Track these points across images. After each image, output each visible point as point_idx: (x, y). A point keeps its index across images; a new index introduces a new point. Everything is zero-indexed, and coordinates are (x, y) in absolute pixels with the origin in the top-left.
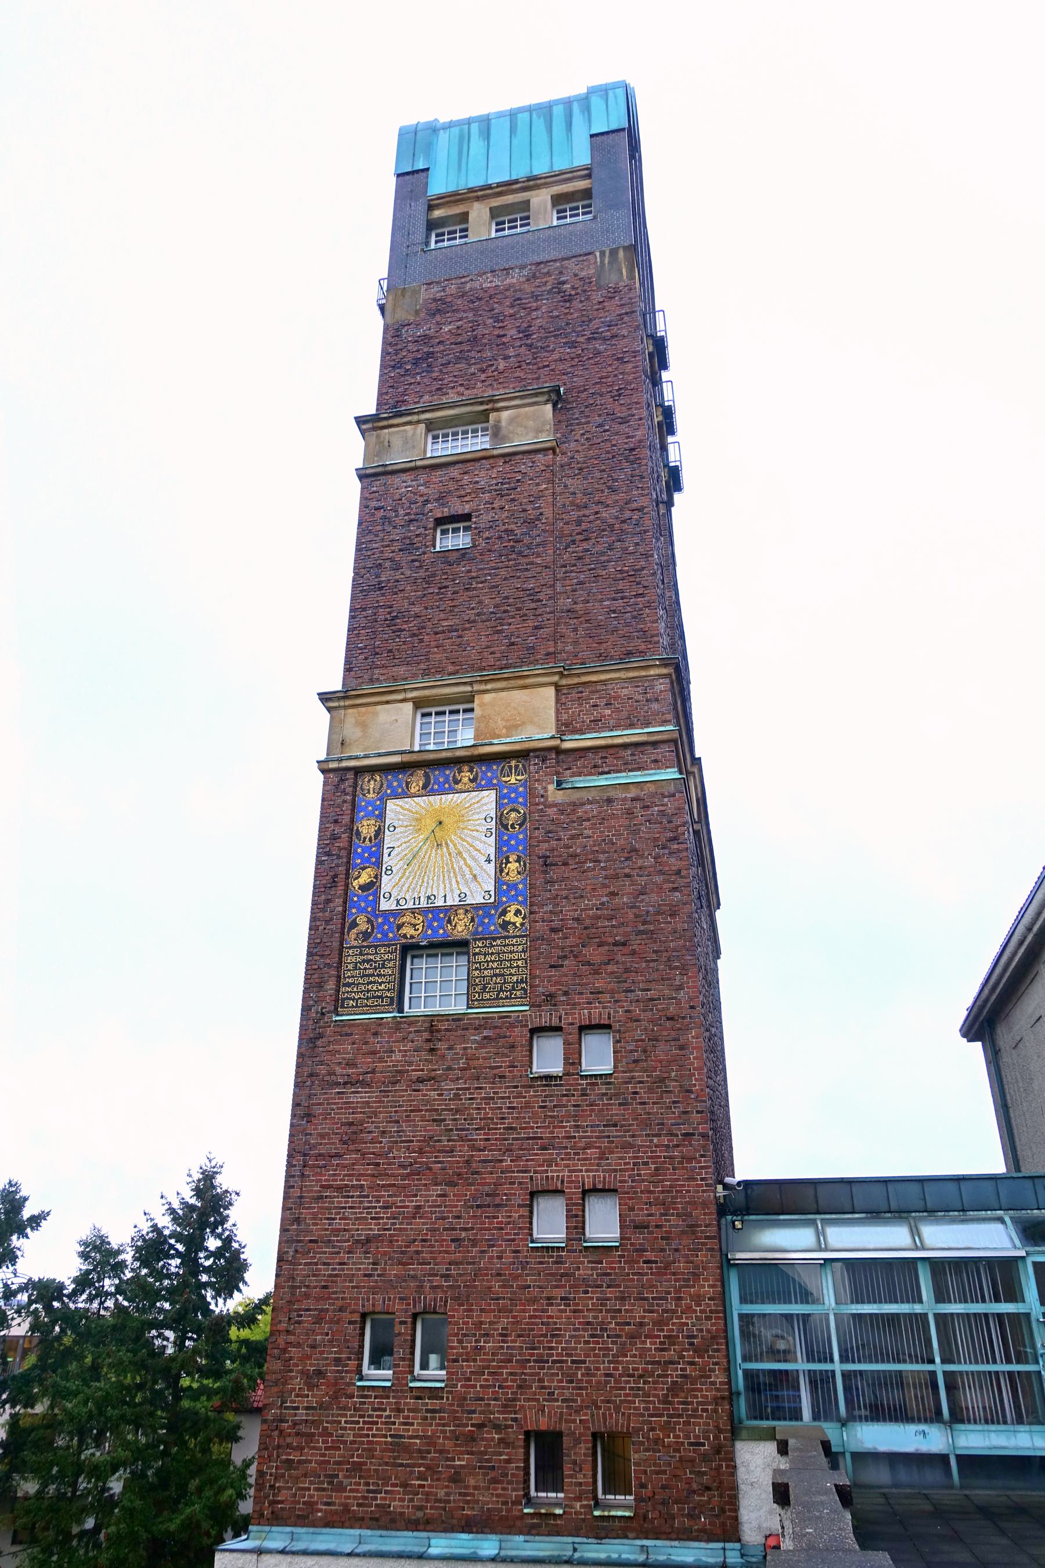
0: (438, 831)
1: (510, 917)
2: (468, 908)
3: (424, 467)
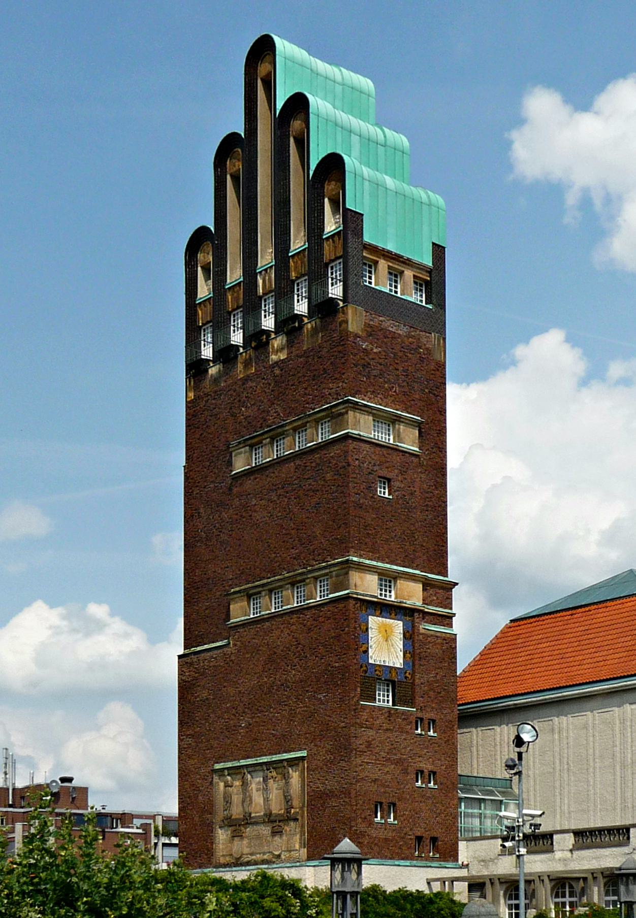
0: (387, 634)
2: (396, 668)
3: (373, 443)
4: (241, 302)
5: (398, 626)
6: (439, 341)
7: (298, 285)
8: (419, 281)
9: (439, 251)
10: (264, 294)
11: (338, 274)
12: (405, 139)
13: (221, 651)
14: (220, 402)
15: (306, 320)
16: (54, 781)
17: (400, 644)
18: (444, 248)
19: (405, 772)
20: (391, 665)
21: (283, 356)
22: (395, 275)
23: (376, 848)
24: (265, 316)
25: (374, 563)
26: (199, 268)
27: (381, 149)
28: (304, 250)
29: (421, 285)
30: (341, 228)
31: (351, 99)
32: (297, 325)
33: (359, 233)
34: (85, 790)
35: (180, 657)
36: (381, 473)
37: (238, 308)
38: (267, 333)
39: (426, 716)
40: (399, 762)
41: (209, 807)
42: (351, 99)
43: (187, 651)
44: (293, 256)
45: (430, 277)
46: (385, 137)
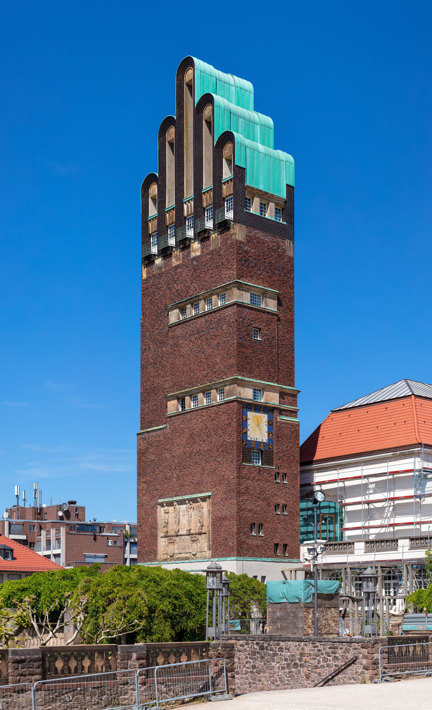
1: (270, 447)
2: (264, 443)
5: (264, 417)
6: (290, 244)
10: (188, 215)
13: (161, 431)
14: (161, 280)
15: (212, 232)
16: (64, 504)
17: (266, 428)
19: (269, 505)
20: (260, 441)
21: (198, 254)
23: (251, 551)
25: (251, 380)
26: (150, 199)
34: (83, 509)
35: (138, 434)
36: (254, 325)
37: (172, 223)
38: (190, 239)
39: (282, 471)
40: (264, 499)
41: (154, 527)
43: (142, 431)
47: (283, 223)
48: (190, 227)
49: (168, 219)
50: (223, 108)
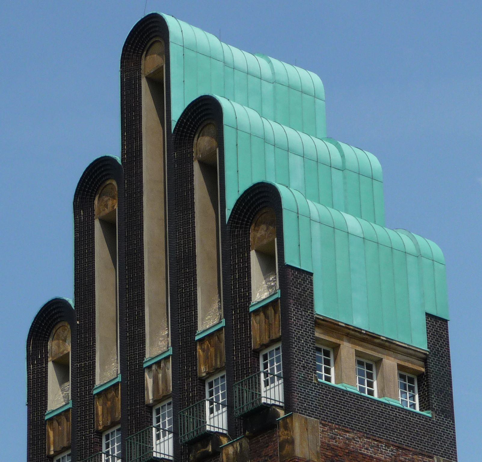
4: (118, 415)
7: (211, 386)
8: (407, 375)
9: (437, 326)
10: (157, 401)
11: (276, 367)
12: (373, 159)
15: (225, 441)
18: (446, 321)
22: (368, 366)
24: (158, 437)
26: (50, 365)
27: (337, 176)
28: (221, 329)
29: (411, 381)
30: (278, 295)
31: (288, 103)
32: (210, 448)
33: (307, 301)
37: (113, 424)
42: (288, 103)
44: (201, 340)
45: (426, 367)
46: (343, 156)
47: (424, 413)
48: (164, 431)
49: (100, 413)
50: (248, 130)
